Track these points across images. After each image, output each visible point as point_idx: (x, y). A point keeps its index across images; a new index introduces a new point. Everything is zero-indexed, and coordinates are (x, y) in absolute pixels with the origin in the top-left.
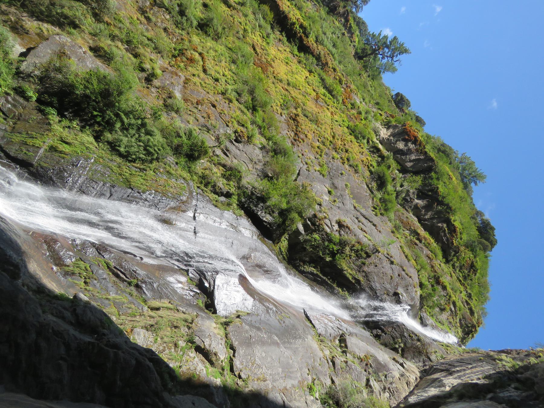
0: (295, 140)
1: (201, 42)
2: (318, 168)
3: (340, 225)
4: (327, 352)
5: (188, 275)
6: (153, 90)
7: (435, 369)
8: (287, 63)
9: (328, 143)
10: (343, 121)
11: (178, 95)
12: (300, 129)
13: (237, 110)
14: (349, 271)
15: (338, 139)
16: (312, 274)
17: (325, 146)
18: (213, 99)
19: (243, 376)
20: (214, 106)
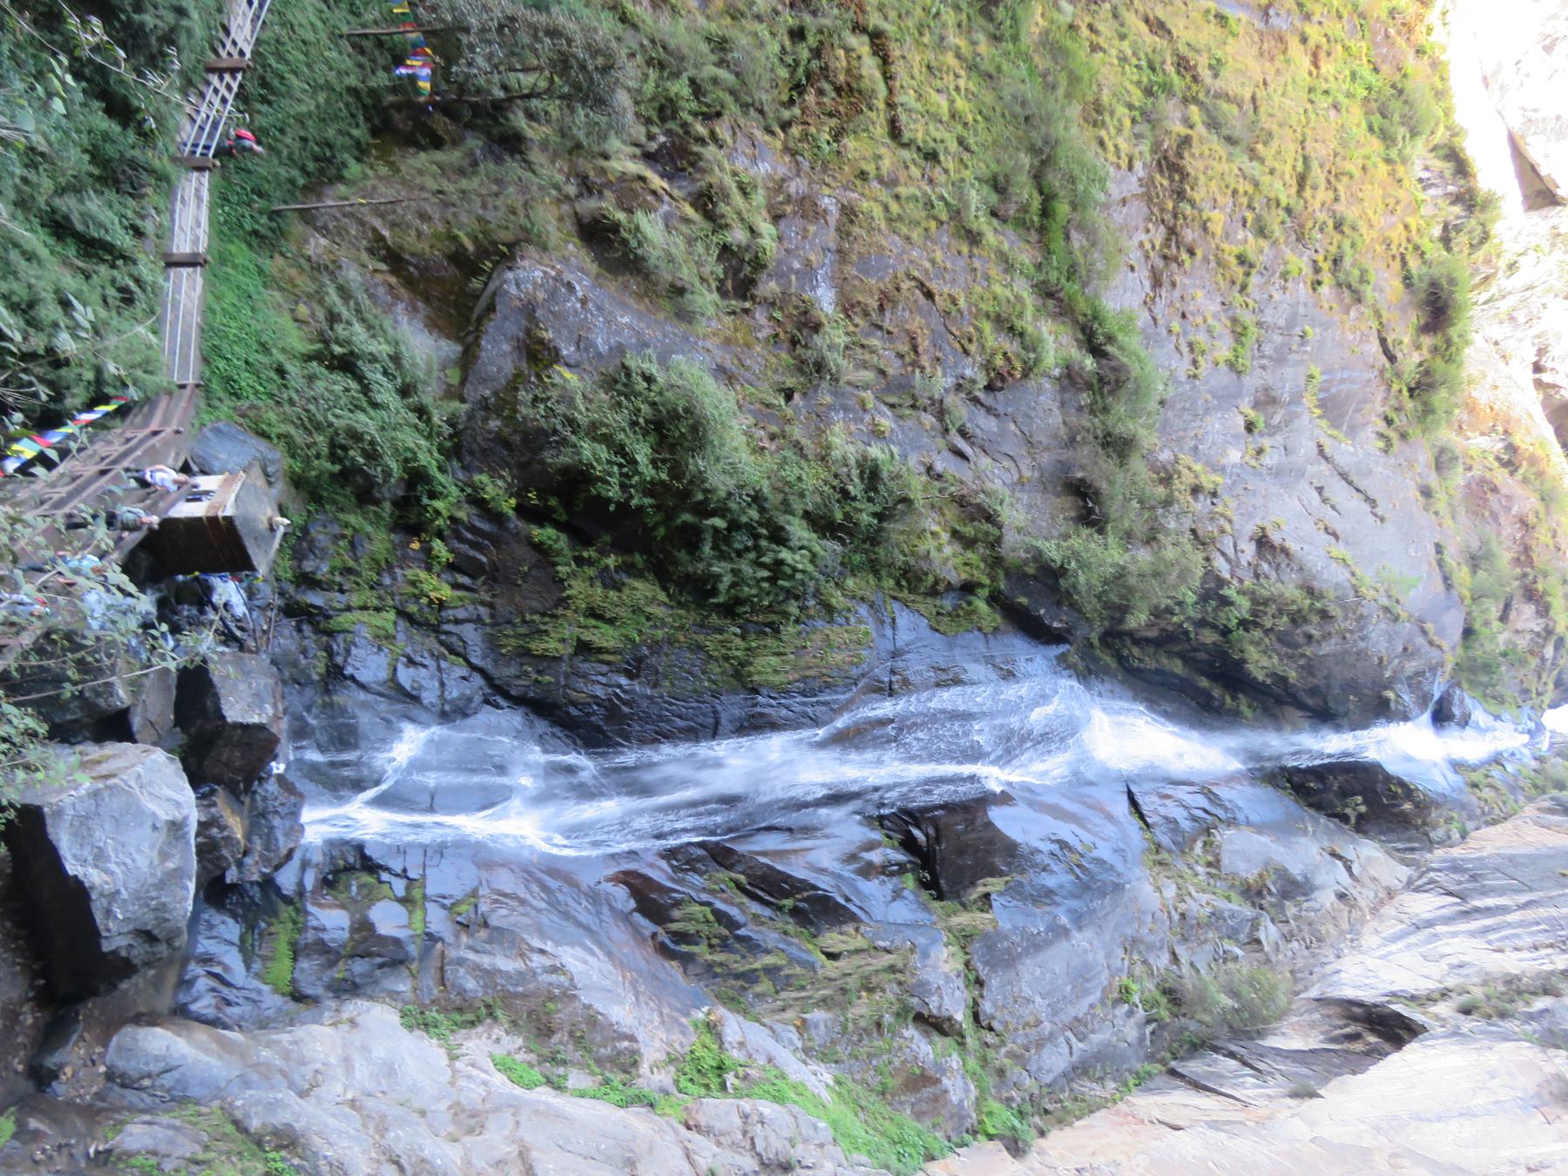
0: (1165, 257)
3: (1262, 542)
4: (1170, 891)
6: (760, 316)
7: (1432, 881)
9: (1275, 219)
13: (995, 271)
14: (1265, 662)
16: (1158, 672)
19: (995, 1024)
20: (929, 295)
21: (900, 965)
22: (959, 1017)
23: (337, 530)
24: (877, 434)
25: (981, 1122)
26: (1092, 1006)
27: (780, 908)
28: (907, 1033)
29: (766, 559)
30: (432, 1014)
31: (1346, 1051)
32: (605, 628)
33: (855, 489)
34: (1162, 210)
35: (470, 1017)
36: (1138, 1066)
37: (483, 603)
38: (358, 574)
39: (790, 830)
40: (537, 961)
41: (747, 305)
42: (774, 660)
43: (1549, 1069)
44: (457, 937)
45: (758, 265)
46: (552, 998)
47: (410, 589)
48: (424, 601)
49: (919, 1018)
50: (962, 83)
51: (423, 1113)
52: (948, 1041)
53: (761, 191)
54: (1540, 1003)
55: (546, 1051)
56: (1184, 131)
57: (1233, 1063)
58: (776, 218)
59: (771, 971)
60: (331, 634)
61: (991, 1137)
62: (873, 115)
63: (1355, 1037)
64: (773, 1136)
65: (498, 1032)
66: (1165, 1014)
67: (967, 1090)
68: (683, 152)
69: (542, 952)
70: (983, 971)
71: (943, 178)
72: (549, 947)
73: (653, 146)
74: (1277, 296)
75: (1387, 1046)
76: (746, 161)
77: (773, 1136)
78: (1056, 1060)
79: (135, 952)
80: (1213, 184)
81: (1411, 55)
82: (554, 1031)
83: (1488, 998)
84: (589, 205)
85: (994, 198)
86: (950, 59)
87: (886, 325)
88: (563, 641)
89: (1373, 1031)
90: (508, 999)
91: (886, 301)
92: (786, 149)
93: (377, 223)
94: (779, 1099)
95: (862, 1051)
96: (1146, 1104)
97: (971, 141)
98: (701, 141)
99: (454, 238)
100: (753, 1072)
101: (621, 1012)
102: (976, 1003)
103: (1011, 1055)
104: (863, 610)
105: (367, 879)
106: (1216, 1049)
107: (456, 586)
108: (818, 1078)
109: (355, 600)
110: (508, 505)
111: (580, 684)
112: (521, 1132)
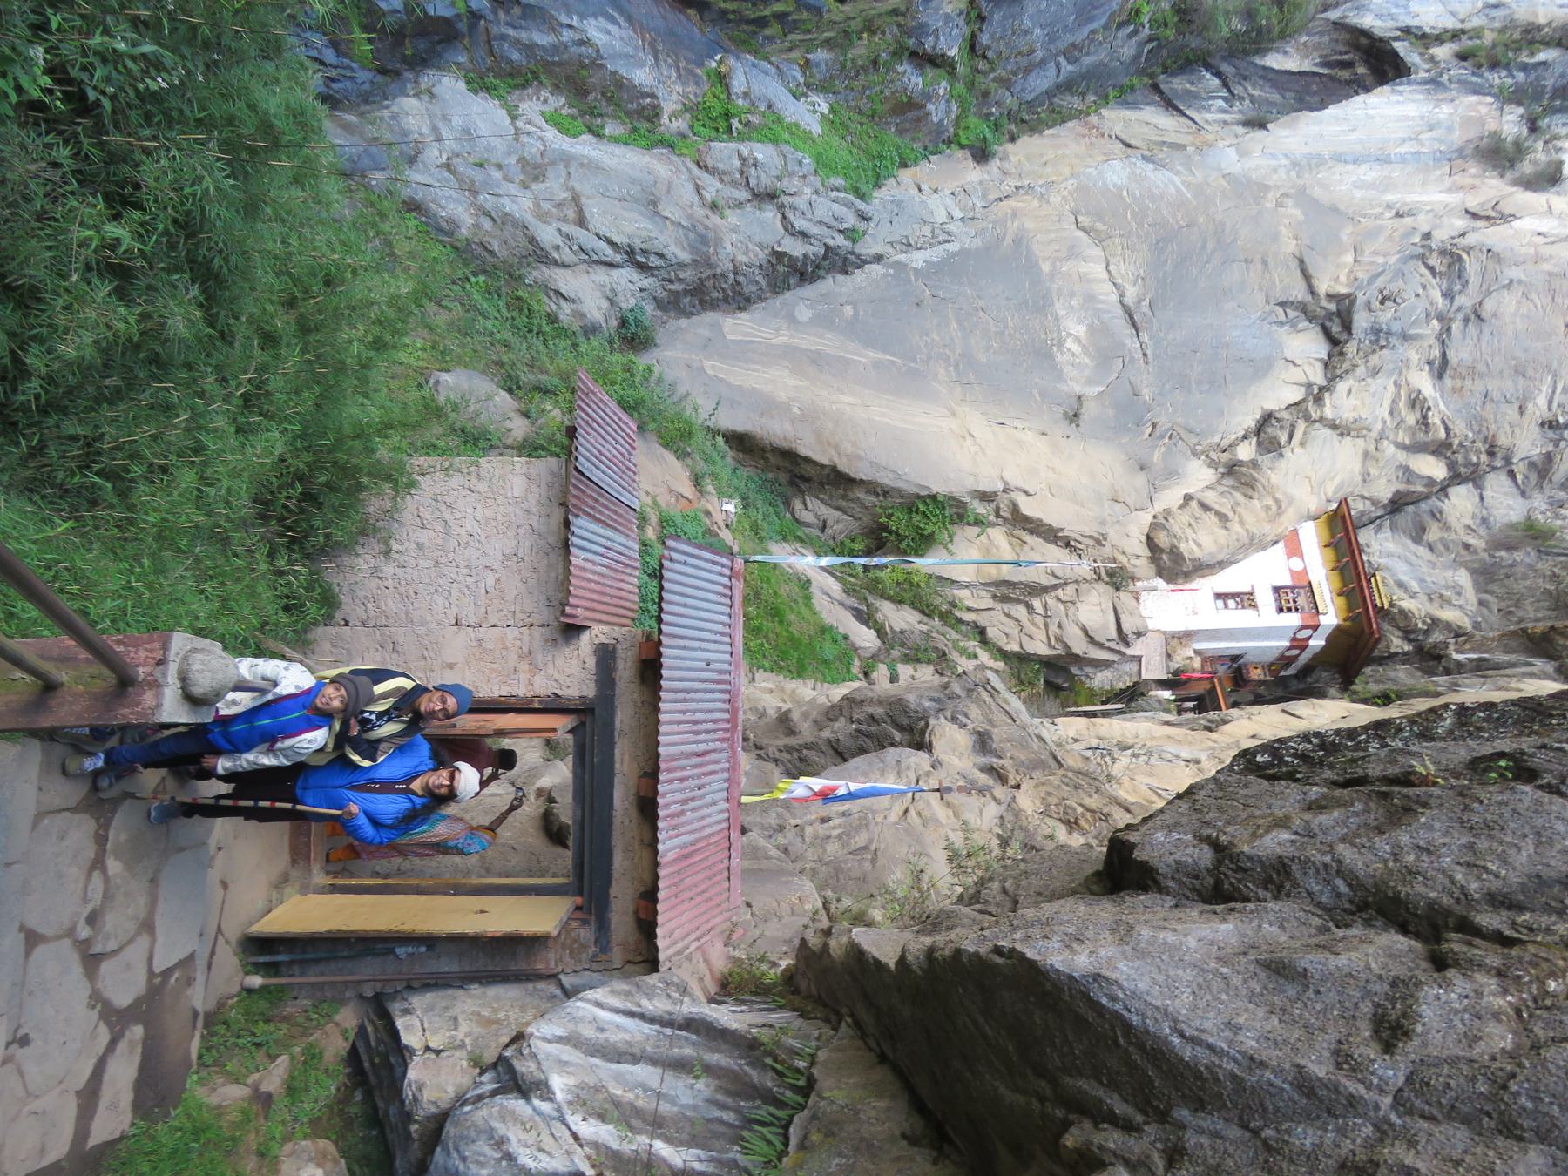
19: (990, 54)
21: (903, 8)
22: (952, 53)
25: (956, 135)
26: (1093, 32)
28: (900, 69)
30: (490, 79)
31: (1332, 78)
35: (519, 81)
36: (1126, 81)
40: (567, 35)
43: (1492, 125)
44: (496, 14)
46: (584, 67)
49: (914, 54)
51: (499, 166)
52: (938, 71)
54: (1541, 56)
55: (584, 107)
57: (1216, 82)
59: (781, 17)
61: (962, 147)
63: (1348, 65)
64: (763, 176)
65: (544, 94)
66: (1170, 33)
67: (948, 111)
69: (570, 26)
70: (986, 8)
75: (1369, 80)
77: (763, 176)
78: (1041, 82)
82: (591, 95)
83: (1494, 46)
89: (1367, 62)
90: (548, 67)
94: (775, 141)
95: (858, 84)
96: (1116, 118)
100: (754, 119)
101: (642, 76)
102: (973, 36)
103: (1001, 81)
106: (1208, 67)
108: (809, 114)
112: (572, 183)
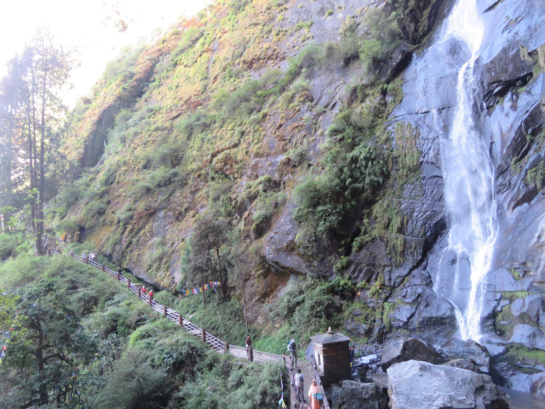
0: (276, 58)
1: (194, 160)
2: (305, 30)
5: (492, 106)
6: (285, 178)
8: (177, 87)
9: (266, 28)
10: (230, 20)
11: (282, 158)
12: (263, 55)
13: (275, 107)
15: (258, 20)
16: (429, 18)
17: (271, 30)
18: (273, 130)
20: (281, 126)
23: (350, 320)
24: (322, 134)
27: (532, 141)
29: (364, 163)
32: (393, 222)
33: (339, 136)
34: (263, 63)
37: (383, 270)
38: (368, 314)
39: (492, 143)
41: (282, 183)
42: (408, 157)
44: (531, 276)
45: (269, 180)
47: (376, 296)
48: (380, 291)
50: (224, 129)
53: (250, 183)
56: (241, 63)
58: (257, 177)
60: (391, 327)
62: (232, 153)
68: (240, 208)
71: (249, 129)
72: (537, 235)
73: (239, 217)
74: (289, 20)
76: (242, 188)
79: (488, 397)
80: (255, 50)
81: (225, 6)
84: (252, 235)
85: (254, 112)
86: (219, 134)
87: (289, 138)
88: (397, 238)
91: (282, 139)
92: (241, 177)
93: (254, 300)
97: (239, 123)
98: (236, 202)
99: (259, 276)
104: (390, 128)
105: (499, 317)
107: (376, 279)
109: (378, 316)
110: (345, 260)
111: (416, 231)
